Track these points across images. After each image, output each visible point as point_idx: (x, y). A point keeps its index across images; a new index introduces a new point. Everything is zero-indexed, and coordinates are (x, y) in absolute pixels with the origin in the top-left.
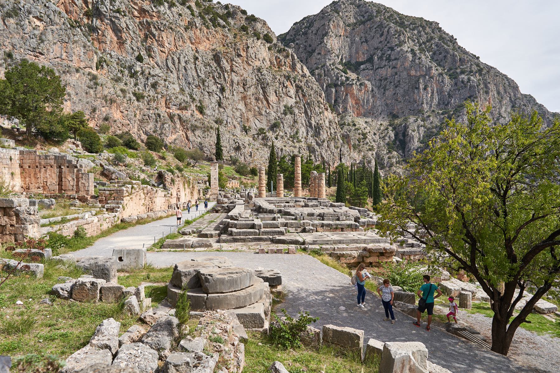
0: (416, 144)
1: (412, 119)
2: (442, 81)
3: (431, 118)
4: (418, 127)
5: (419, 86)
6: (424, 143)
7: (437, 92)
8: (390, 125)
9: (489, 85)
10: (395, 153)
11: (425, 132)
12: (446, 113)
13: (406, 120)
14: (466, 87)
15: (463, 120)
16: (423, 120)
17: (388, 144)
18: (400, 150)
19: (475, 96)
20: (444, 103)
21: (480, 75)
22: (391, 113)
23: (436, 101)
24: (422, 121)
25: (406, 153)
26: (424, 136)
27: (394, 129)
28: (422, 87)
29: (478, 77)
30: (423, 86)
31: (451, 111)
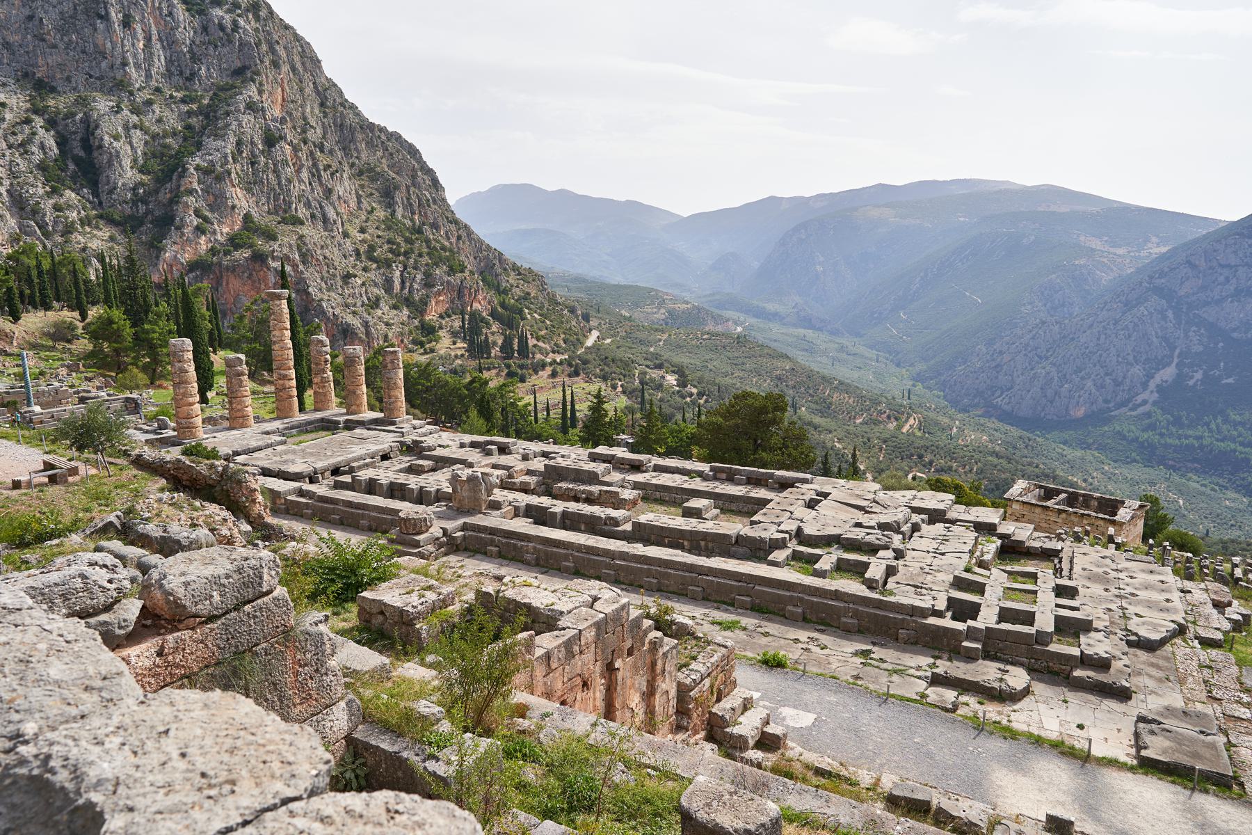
0: (127, 174)
1: (102, 104)
2: (170, 14)
3: (156, 107)
4: (126, 128)
5: (107, 13)
6: (149, 173)
7: (160, 39)
8: (36, 111)
9: (277, 48)
10: (70, 195)
11: (146, 143)
12: (193, 101)
13: (83, 102)
14: (230, 42)
15: (240, 125)
16: (135, 111)
17: (42, 167)
18: (82, 186)
19: (253, 68)
20: (181, 73)
21: (257, 18)
22: (26, 75)
23: (160, 63)
24: (132, 113)
25: (104, 197)
26: (145, 154)
27: (51, 124)
28: (115, 16)
29: (253, 23)
30: (120, 16)
31: (202, 97)
